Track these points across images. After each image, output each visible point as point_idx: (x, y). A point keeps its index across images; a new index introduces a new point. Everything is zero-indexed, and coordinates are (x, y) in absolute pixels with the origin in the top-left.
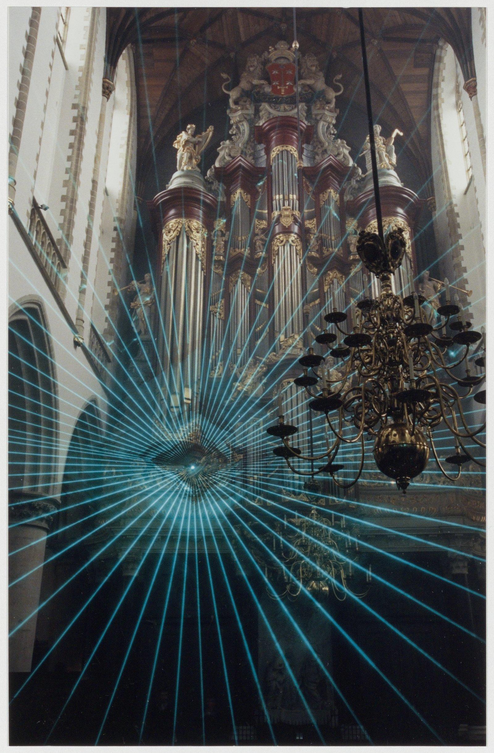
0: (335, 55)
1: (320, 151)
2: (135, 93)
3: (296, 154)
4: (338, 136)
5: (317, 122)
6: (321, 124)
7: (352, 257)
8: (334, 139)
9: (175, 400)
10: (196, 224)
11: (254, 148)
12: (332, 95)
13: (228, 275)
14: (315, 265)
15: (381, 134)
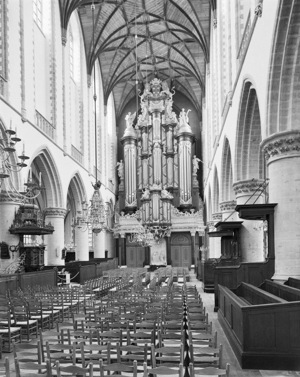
0: (172, 80)
1: (167, 117)
2: (113, 98)
3: (160, 120)
4: (173, 111)
5: (167, 106)
6: (168, 107)
7: (175, 153)
8: (172, 112)
9: (130, 196)
10: (133, 145)
11: (148, 117)
12: (171, 95)
13: (142, 160)
14: (165, 155)
15: (184, 111)
